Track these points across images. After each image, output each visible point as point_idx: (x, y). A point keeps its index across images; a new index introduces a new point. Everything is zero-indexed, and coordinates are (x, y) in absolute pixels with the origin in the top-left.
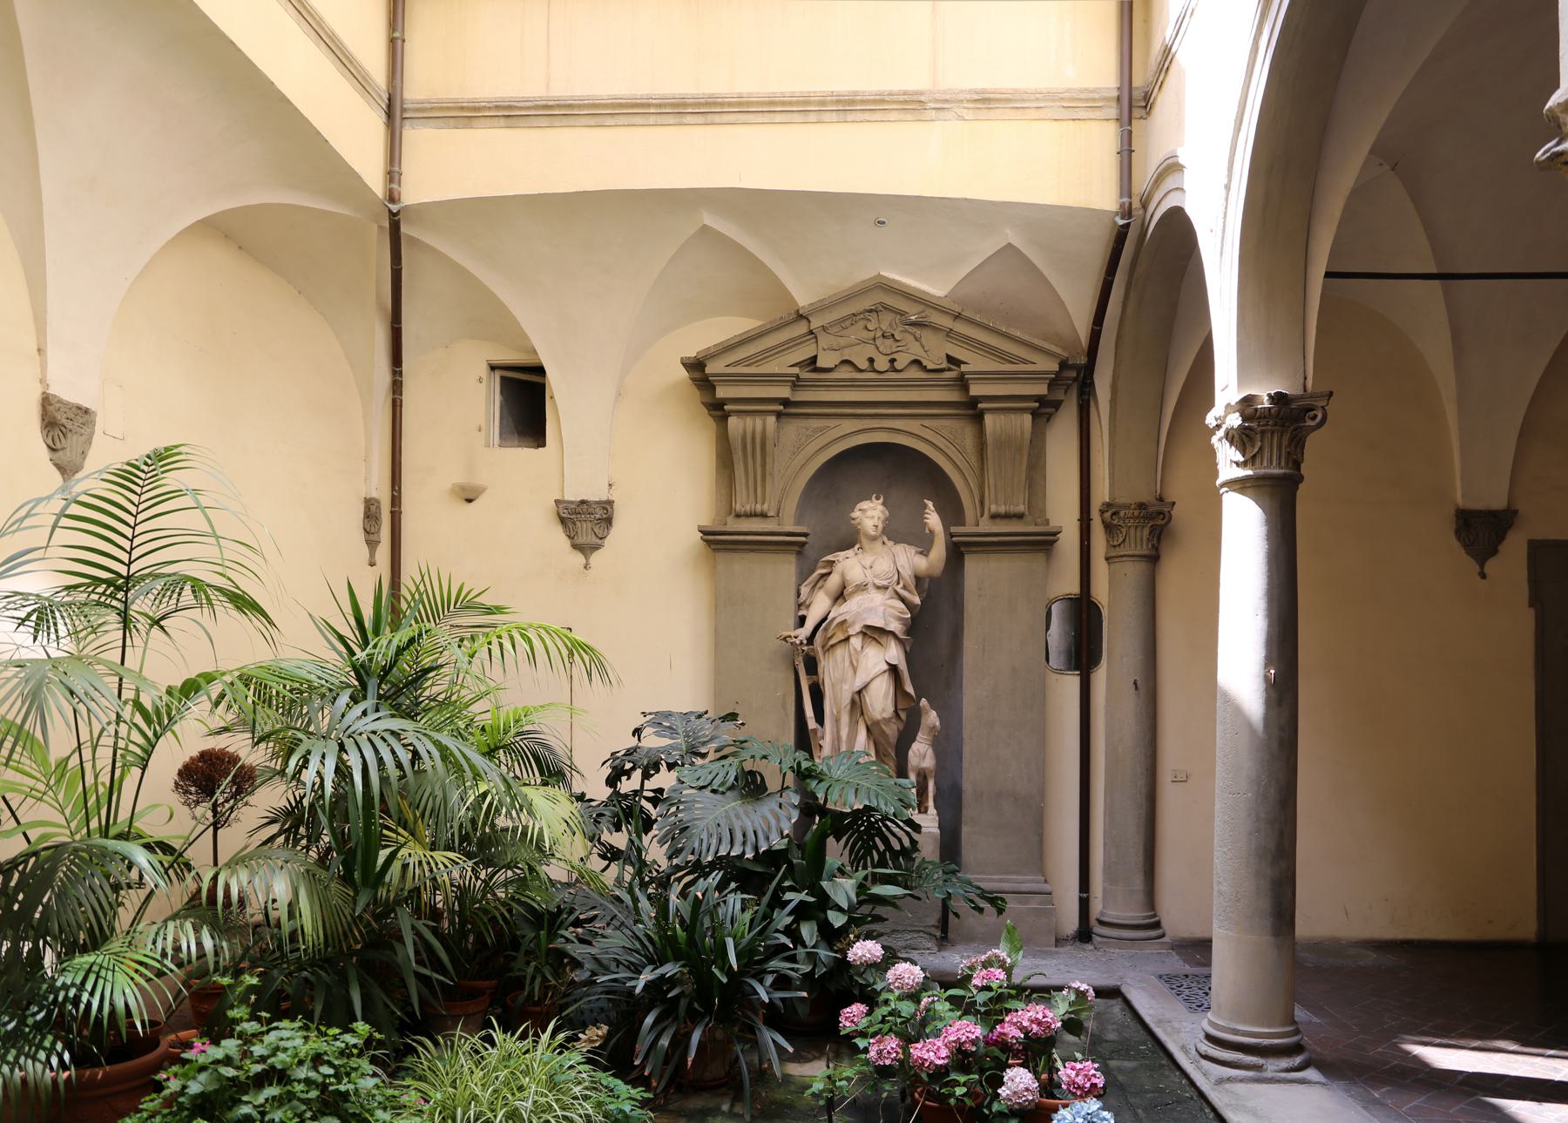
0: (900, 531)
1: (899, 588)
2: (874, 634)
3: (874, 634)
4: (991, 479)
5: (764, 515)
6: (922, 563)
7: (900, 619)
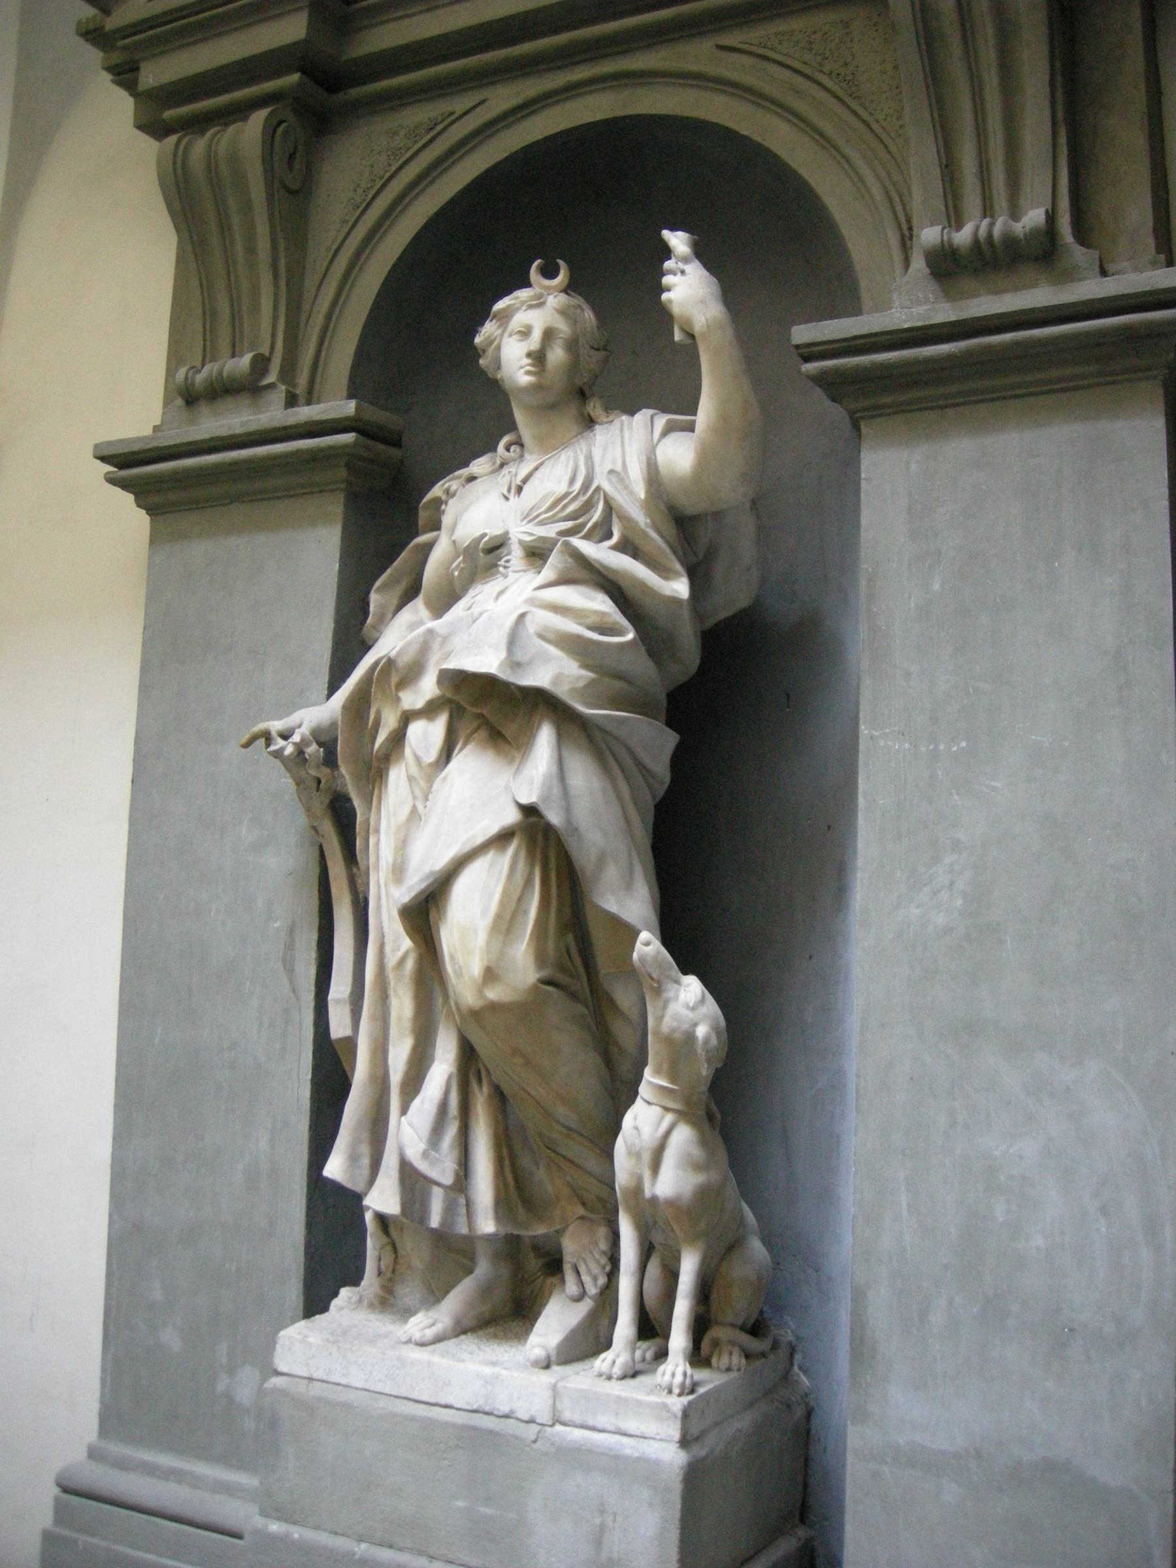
0: (624, 366)
2: (489, 709)
3: (489, 709)
6: (679, 455)
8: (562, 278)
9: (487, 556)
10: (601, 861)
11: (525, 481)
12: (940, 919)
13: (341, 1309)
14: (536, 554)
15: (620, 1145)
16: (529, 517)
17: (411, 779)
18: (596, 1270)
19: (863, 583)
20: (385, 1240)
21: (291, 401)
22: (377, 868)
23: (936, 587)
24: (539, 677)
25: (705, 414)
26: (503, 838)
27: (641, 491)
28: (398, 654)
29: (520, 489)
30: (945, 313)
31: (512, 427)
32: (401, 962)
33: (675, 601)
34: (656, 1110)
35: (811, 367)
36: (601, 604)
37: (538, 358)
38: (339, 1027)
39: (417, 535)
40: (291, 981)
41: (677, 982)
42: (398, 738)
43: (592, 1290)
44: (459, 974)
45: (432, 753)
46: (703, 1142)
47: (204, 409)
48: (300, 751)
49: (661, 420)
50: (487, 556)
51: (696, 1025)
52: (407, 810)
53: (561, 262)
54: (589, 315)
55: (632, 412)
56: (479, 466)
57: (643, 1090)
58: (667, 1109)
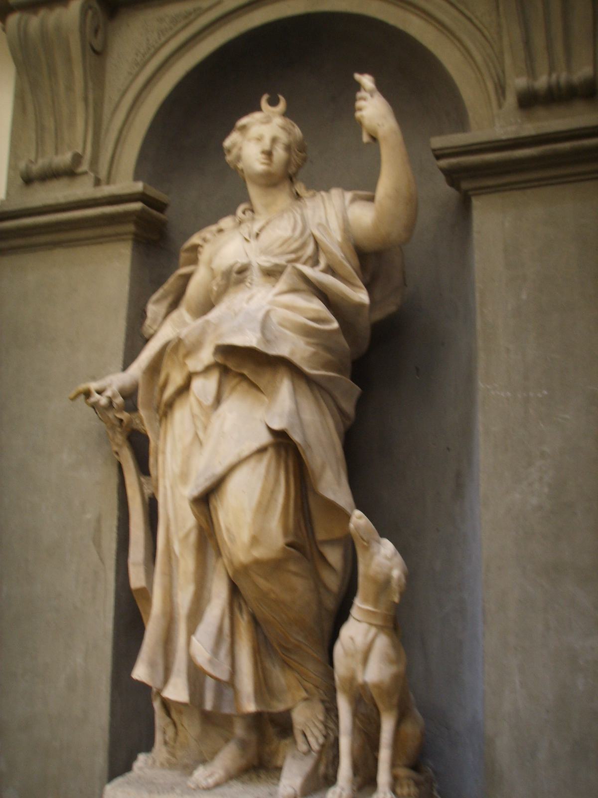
1: (315, 273)
4: (501, 8)
5: (70, 173)
6: (364, 216)
7: (307, 332)
8: (282, 106)
9: (238, 276)
10: (323, 467)
11: (261, 230)
12: (534, 501)
13: (141, 769)
14: (272, 273)
15: (339, 650)
16: (265, 252)
17: (193, 416)
18: (317, 733)
19: (477, 295)
20: (168, 720)
21: (97, 182)
22: (164, 477)
23: (524, 296)
24: (282, 350)
25: (385, 185)
26: (262, 450)
27: (338, 236)
28: (186, 336)
29: (257, 235)
30: (529, 129)
31: (246, 199)
32: (187, 536)
33: (361, 306)
34: (364, 626)
35: (444, 163)
36: (317, 306)
37: (269, 154)
38: (137, 580)
39: (177, 267)
40: (99, 553)
41: (379, 542)
42: (185, 388)
43: (315, 747)
44: (233, 540)
45: (209, 399)
46: (395, 646)
47: (37, 186)
48: (111, 402)
49: (349, 195)
50: (238, 276)
51: (391, 569)
52: (189, 438)
53: (281, 98)
54: (297, 131)
55: (327, 190)
56: (226, 223)
57: (354, 612)
58: (371, 624)
